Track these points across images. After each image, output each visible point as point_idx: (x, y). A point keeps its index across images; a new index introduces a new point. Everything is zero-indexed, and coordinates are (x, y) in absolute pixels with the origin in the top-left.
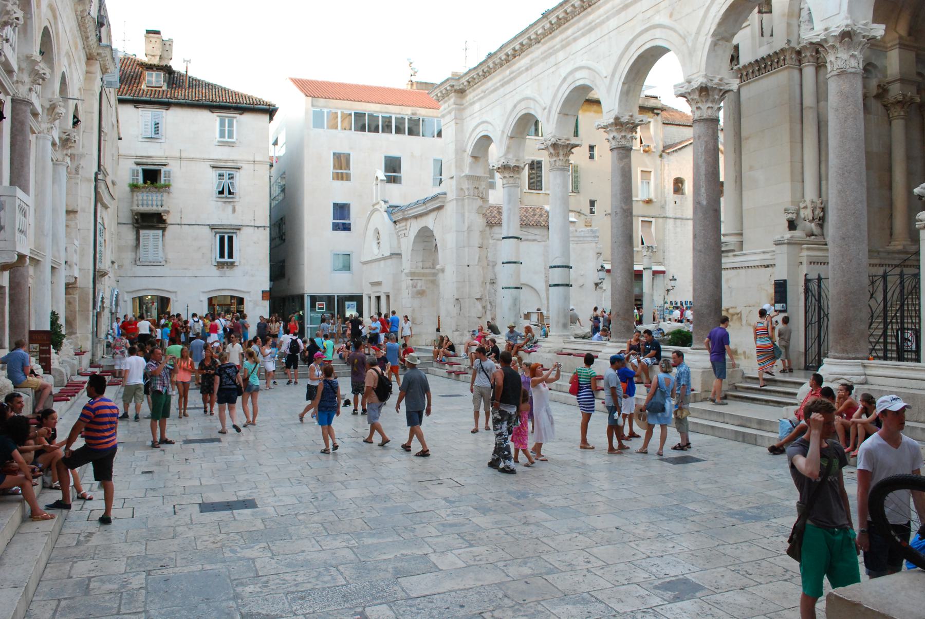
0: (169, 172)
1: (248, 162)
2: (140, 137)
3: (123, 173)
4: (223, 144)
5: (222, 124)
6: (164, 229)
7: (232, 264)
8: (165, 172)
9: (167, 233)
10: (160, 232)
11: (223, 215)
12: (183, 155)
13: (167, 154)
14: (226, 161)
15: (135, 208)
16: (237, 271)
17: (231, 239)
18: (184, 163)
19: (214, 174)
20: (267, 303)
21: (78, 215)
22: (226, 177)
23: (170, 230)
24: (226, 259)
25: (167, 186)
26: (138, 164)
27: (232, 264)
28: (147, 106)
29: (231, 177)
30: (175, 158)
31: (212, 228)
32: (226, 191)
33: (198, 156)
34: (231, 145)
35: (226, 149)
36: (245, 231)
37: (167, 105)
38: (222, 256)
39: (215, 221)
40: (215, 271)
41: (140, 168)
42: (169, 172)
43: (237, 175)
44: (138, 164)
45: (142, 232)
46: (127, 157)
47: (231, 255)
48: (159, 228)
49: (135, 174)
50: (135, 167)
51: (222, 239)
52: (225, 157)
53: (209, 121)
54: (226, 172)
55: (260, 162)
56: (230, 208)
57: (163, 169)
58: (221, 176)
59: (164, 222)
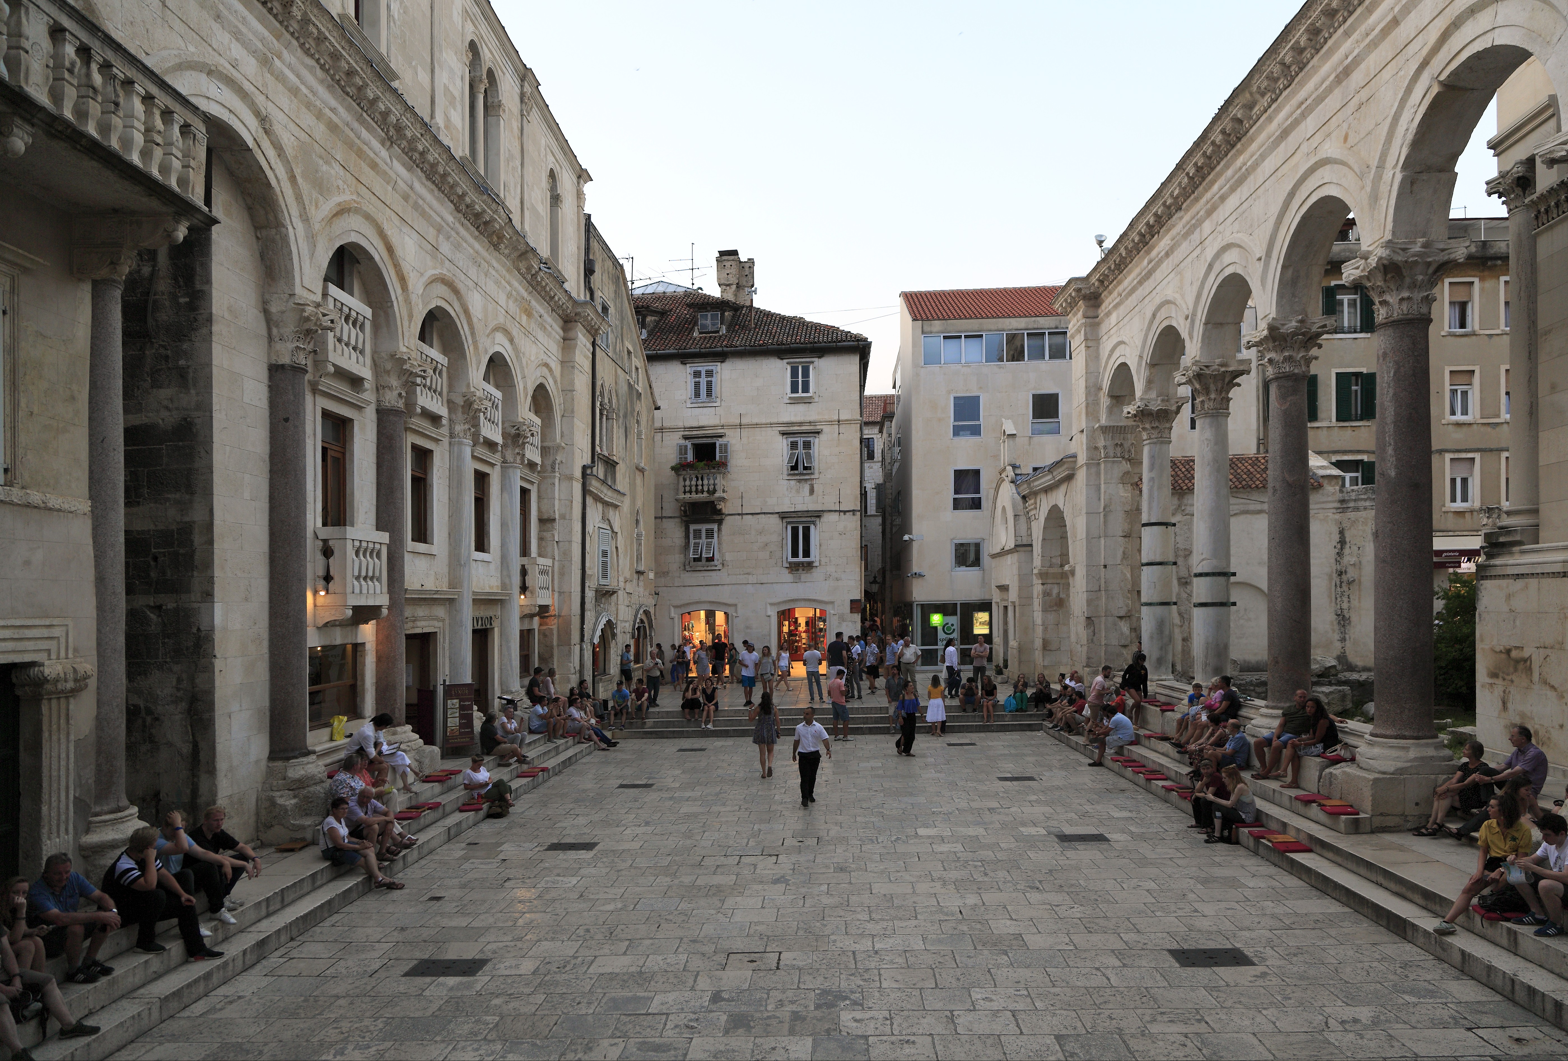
0: (726, 445)
1: (830, 423)
2: (689, 401)
3: (670, 449)
4: (794, 402)
5: (794, 374)
7: (809, 566)
8: (721, 445)
10: (715, 527)
11: (794, 498)
12: (744, 421)
13: (723, 422)
14: (801, 424)
15: (682, 496)
16: (817, 574)
17: (807, 531)
18: (745, 432)
19: (782, 445)
20: (857, 617)
21: (557, 525)
22: (800, 445)
23: (728, 522)
24: (801, 559)
25: (724, 464)
26: (686, 438)
27: (809, 566)
28: (697, 360)
29: (807, 445)
30: (733, 427)
31: (783, 516)
32: (800, 467)
33: (764, 421)
34: (808, 401)
35: (801, 408)
36: (828, 518)
37: (722, 356)
38: (795, 554)
39: (786, 508)
40: (787, 576)
41: (689, 443)
42: (726, 445)
43: (818, 444)
44: (686, 438)
45: (692, 527)
46: (673, 430)
47: (807, 554)
48: (714, 521)
49: (682, 450)
50: (682, 442)
51: (795, 531)
52: (799, 419)
53: (775, 372)
54: (800, 440)
55: (849, 422)
56: (807, 487)
57: (719, 442)
58: (794, 446)
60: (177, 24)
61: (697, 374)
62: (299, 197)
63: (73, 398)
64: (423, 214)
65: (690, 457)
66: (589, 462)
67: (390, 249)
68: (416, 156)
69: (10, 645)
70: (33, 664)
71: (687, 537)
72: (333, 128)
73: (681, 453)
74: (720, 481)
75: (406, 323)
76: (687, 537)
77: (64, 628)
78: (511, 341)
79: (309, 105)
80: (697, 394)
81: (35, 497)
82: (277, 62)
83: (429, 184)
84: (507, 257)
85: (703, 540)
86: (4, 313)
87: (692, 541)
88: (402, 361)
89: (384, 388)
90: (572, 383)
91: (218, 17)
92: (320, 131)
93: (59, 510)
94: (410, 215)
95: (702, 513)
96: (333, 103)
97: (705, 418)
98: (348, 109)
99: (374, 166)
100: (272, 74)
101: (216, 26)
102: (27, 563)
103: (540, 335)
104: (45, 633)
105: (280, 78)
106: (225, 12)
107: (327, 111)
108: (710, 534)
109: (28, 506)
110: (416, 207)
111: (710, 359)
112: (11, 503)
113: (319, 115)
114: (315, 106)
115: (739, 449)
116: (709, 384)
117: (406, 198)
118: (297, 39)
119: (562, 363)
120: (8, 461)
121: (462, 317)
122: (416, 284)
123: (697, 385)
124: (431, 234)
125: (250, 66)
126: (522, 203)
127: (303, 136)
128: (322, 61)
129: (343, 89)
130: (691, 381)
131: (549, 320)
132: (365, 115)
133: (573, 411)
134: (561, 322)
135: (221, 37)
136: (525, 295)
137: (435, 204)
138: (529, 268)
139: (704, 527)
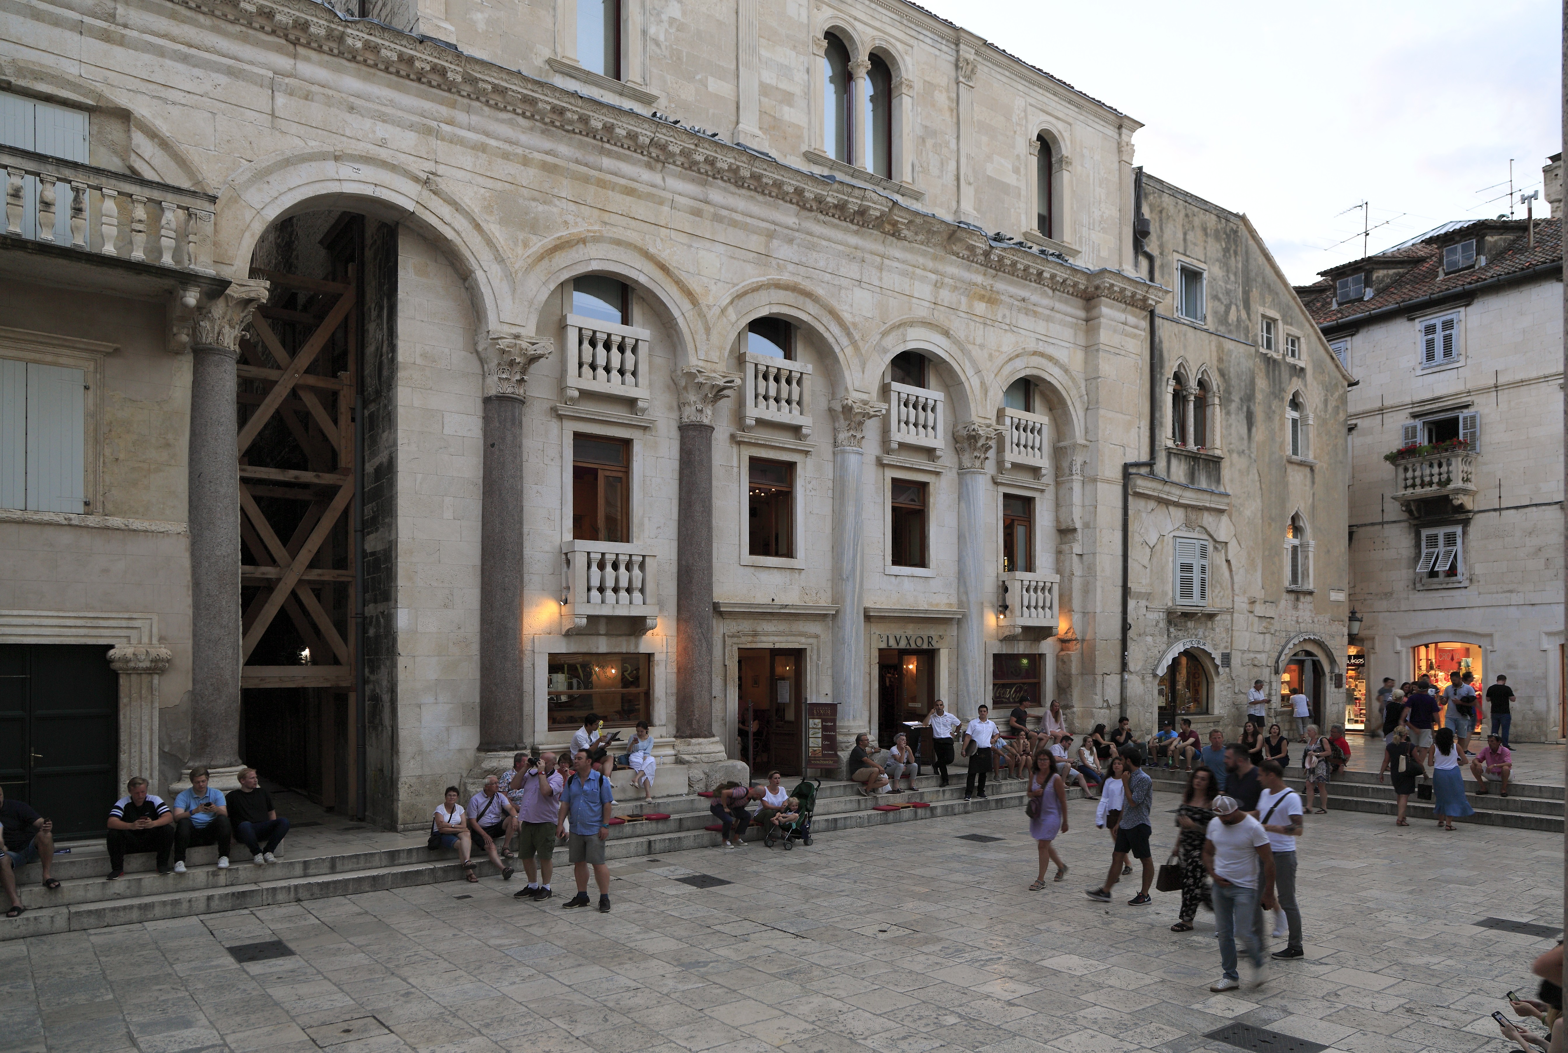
0: (1473, 418)
2: (1419, 368)
6: (1466, 523)
8: (1465, 419)
9: (1472, 529)
10: (1458, 530)
12: (1502, 380)
13: (1469, 386)
15: (1401, 492)
18: (1503, 396)
23: (1478, 524)
26: (1415, 416)
28: (1428, 311)
33: (1534, 375)
37: (1466, 297)
41: (1418, 423)
42: (1473, 418)
44: (1415, 416)
45: (1425, 533)
48: (1456, 522)
49: (1410, 432)
50: (1411, 422)
57: (1462, 415)
59: (1461, 508)
60: (294, 128)
61: (1430, 330)
62: (489, 242)
63: (168, 445)
64: (734, 224)
65: (1422, 439)
66: (1145, 457)
67: (663, 268)
68: (704, 167)
69: (82, 631)
70: (112, 647)
71: (1418, 545)
72: (549, 169)
73: (1406, 437)
74: (1457, 467)
75: (701, 336)
76: (1418, 545)
77: (148, 621)
78: (946, 333)
79: (506, 156)
80: (1430, 356)
81: (116, 521)
82: (445, 128)
83: (743, 192)
84: (926, 243)
85: (1441, 548)
86: (86, 388)
87: (1424, 551)
88: (691, 376)
89: (684, 404)
90: (1096, 368)
91: (352, 109)
92: (529, 176)
93: (146, 531)
94: (705, 228)
95: (1437, 512)
96: (547, 145)
97: (1443, 385)
98: (582, 146)
99: (630, 192)
100: (443, 140)
101: (350, 118)
102: (106, 571)
103: (1024, 321)
104: (124, 623)
105: (461, 142)
106: (358, 102)
107: (537, 156)
108: (1450, 540)
109: (107, 528)
110: (717, 218)
111: (1447, 306)
112: (87, 527)
113: (526, 162)
114: (516, 154)
115: (1492, 419)
116: (1448, 340)
117: (697, 213)
118: (478, 99)
119: (1086, 348)
120: (90, 496)
121: (826, 319)
122: (716, 295)
123: (1430, 344)
124: (755, 242)
125: (408, 140)
126: (958, 179)
127: (499, 186)
128: (519, 111)
129: (562, 127)
130: (1421, 340)
131: (1045, 302)
132: (607, 146)
133: (1097, 402)
134: (1080, 302)
135: (357, 124)
136: (979, 279)
137: (755, 209)
138: (972, 249)
139: (1441, 532)
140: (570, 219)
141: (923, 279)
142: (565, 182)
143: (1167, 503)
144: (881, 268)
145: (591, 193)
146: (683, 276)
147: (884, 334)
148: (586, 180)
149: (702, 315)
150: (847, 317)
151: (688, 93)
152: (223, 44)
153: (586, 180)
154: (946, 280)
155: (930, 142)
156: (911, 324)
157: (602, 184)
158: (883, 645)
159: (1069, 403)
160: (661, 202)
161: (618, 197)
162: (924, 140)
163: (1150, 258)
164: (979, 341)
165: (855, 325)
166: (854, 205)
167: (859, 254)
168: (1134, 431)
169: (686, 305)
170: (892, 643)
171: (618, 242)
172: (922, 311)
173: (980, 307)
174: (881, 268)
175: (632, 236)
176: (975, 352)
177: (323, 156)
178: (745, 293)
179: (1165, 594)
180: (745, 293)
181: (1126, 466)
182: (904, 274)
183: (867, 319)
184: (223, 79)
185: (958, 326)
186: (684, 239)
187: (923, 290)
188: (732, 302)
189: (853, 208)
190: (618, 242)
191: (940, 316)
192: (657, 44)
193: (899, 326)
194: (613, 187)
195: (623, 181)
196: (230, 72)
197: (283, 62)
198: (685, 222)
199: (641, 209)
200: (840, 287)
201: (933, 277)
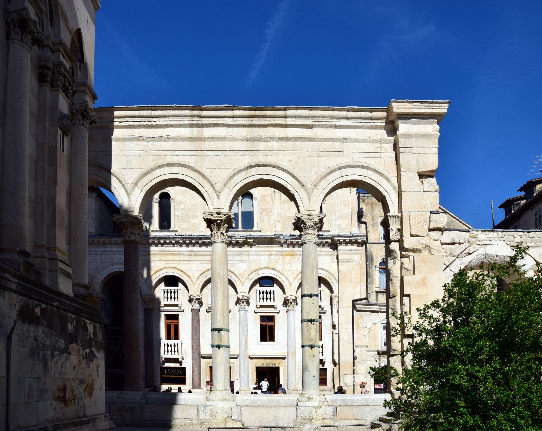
64: (201, 255)
78: (274, 269)
94: (193, 258)
110: (196, 255)
138: (279, 242)
140: (159, 265)
141: (264, 255)
142: (158, 256)
143: (377, 312)
144: (248, 255)
145: (164, 257)
146: (186, 272)
147: (249, 275)
148: (162, 255)
149: (192, 281)
150: (236, 272)
151: (186, 226)
152: (94, 249)
153: (162, 255)
154: (273, 253)
155: (264, 214)
156: (260, 269)
157: (166, 254)
158: (257, 366)
159: (330, 282)
160: (181, 255)
161: (170, 256)
162: (262, 213)
163: (365, 223)
164: (288, 269)
165: (240, 274)
166: (234, 242)
167: (240, 253)
168: (358, 288)
169: (188, 279)
170: (261, 365)
171: (170, 268)
172: (264, 265)
173: (288, 258)
174: (248, 255)
175: (174, 265)
176: (286, 273)
177: (110, 266)
178: (204, 272)
179: (378, 345)
180: (204, 272)
181: (353, 301)
182: (256, 255)
183: (244, 271)
184: (94, 256)
185: (279, 267)
186: (187, 262)
187: (266, 258)
188: (200, 275)
189: (234, 242)
190: (170, 268)
191: (271, 265)
192: (178, 216)
193: (255, 271)
194: (169, 254)
195: (170, 253)
196: (95, 254)
197: (103, 249)
198: (187, 258)
199: (176, 258)
200: (235, 264)
201: (268, 253)
